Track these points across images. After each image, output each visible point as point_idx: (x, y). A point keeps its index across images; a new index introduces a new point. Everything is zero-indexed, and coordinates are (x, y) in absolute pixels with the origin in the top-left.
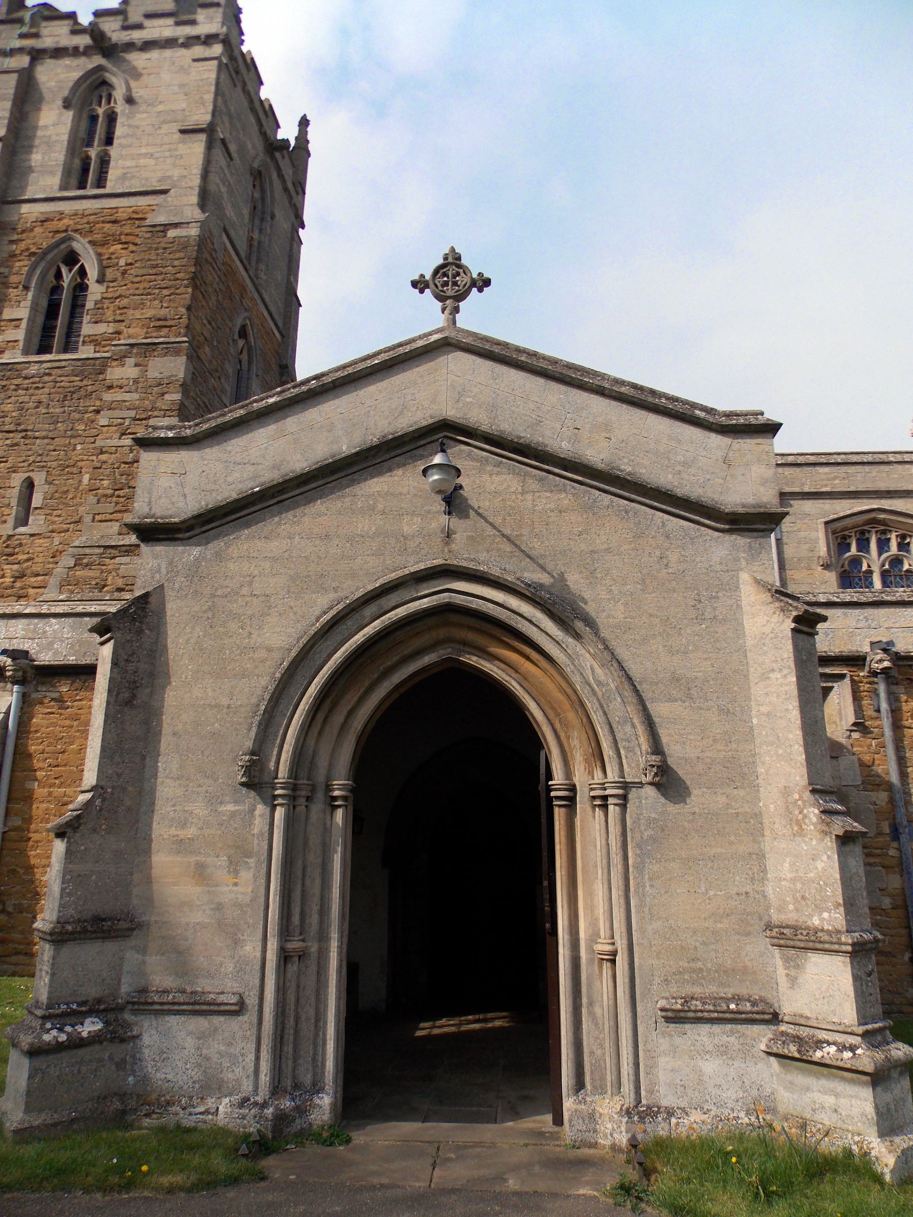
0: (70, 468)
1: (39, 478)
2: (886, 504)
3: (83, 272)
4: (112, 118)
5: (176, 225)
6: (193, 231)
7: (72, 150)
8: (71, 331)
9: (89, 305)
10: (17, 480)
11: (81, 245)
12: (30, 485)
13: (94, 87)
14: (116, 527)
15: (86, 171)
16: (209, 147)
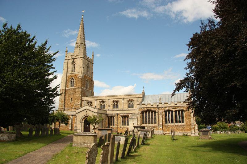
2: (131, 99)
4: (75, 64)
6: (81, 77)
8: (73, 85)
13: (73, 62)
15: (73, 70)
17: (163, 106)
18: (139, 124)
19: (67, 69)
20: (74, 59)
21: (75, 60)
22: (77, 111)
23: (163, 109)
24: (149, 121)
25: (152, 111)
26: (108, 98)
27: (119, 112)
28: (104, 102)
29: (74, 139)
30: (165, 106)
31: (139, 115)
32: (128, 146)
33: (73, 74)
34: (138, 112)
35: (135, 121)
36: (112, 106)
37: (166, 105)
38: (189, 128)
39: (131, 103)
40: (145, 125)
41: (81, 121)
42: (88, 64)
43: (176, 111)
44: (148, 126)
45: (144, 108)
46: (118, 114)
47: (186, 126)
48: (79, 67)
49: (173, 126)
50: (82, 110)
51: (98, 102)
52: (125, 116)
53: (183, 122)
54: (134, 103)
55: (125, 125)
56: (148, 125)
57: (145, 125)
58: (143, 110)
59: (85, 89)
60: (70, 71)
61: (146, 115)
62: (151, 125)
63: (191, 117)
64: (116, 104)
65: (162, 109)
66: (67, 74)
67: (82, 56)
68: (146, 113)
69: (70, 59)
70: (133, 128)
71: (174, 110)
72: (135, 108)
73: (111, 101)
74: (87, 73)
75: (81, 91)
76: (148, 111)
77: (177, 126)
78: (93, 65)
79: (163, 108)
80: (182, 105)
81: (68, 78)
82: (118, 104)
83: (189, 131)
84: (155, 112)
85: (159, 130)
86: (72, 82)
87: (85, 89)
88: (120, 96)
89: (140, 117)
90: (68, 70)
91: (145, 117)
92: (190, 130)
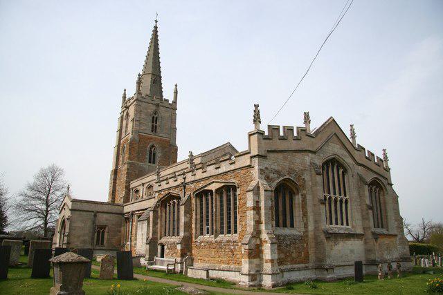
24: (229, 227)
43: (219, 191)
49: (210, 243)
66: (120, 139)
75: (128, 169)
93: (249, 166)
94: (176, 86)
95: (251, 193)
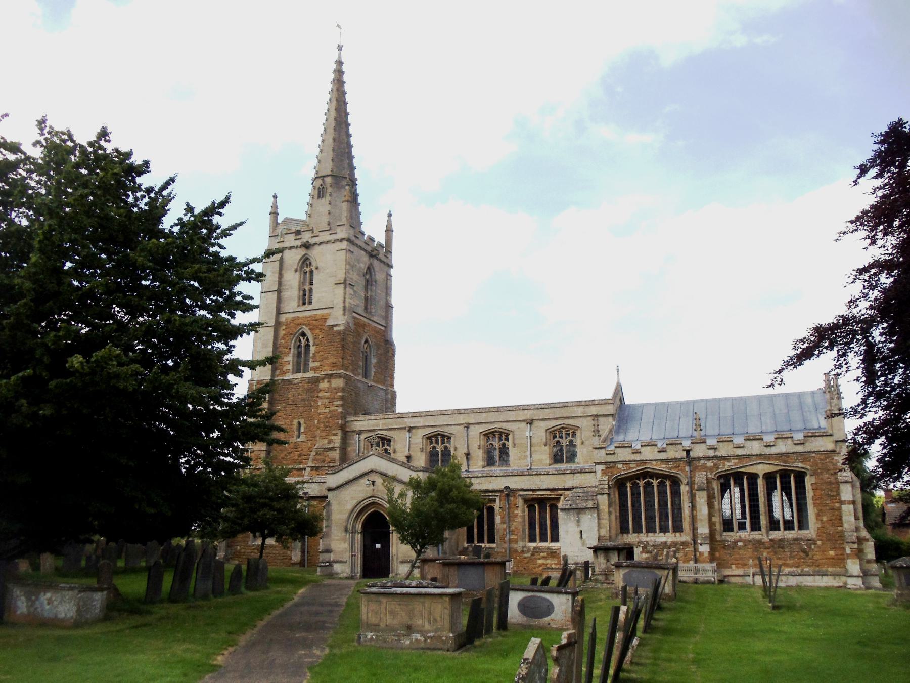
0: (310, 418)
1: (302, 421)
3: (308, 340)
4: (312, 272)
5: (336, 325)
7: (299, 289)
8: (306, 364)
9: (311, 355)
10: (295, 422)
11: (306, 330)
12: (299, 423)
13: (305, 261)
14: (326, 441)
15: (306, 297)
16: (345, 288)
17: (711, 453)
18: (604, 532)
19: (279, 292)
20: (307, 246)
21: (316, 254)
22: (333, 480)
23: (711, 470)
24: (650, 519)
25: (663, 477)
26: (462, 419)
27: (514, 483)
28: (445, 438)
29: (364, 609)
30: (718, 454)
31: (606, 497)
32: (619, 636)
33: (306, 313)
34: (597, 479)
35: (589, 521)
36: (479, 456)
37: (724, 450)
38: (832, 553)
39: (564, 442)
40: (631, 538)
41: (350, 528)
42: (368, 268)
43: (769, 478)
44: (646, 542)
45: (625, 463)
46: (508, 493)
47: (819, 543)
48: (333, 280)
49: (760, 542)
50: (351, 477)
51: (418, 438)
52: (542, 501)
53: (803, 525)
54: (577, 441)
55: (543, 539)
56: (644, 537)
57: (631, 538)
58: (622, 470)
59: (360, 378)
60: (291, 303)
61: (636, 495)
62: (660, 538)
63: (842, 503)
64: (497, 443)
65: (705, 468)
66: (279, 312)
67: (342, 233)
68: (635, 486)
69: (291, 248)
70: (589, 556)
71: (761, 469)
72: (581, 461)
73: (476, 431)
74: (366, 308)
76: (646, 474)
77: (778, 545)
78: (393, 272)
79: (710, 464)
80: (800, 449)
81: (282, 333)
82: (510, 444)
83: (833, 566)
84: (676, 482)
85: (696, 561)
86: (302, 353)
87: (360, 378)
88: (517, 408)
89: (610, 505)
90: (286, 294)
91: (633, 506)
92: (840, 560)
93: (833, 452)
94: (390, 215)
95: (849, 486)
